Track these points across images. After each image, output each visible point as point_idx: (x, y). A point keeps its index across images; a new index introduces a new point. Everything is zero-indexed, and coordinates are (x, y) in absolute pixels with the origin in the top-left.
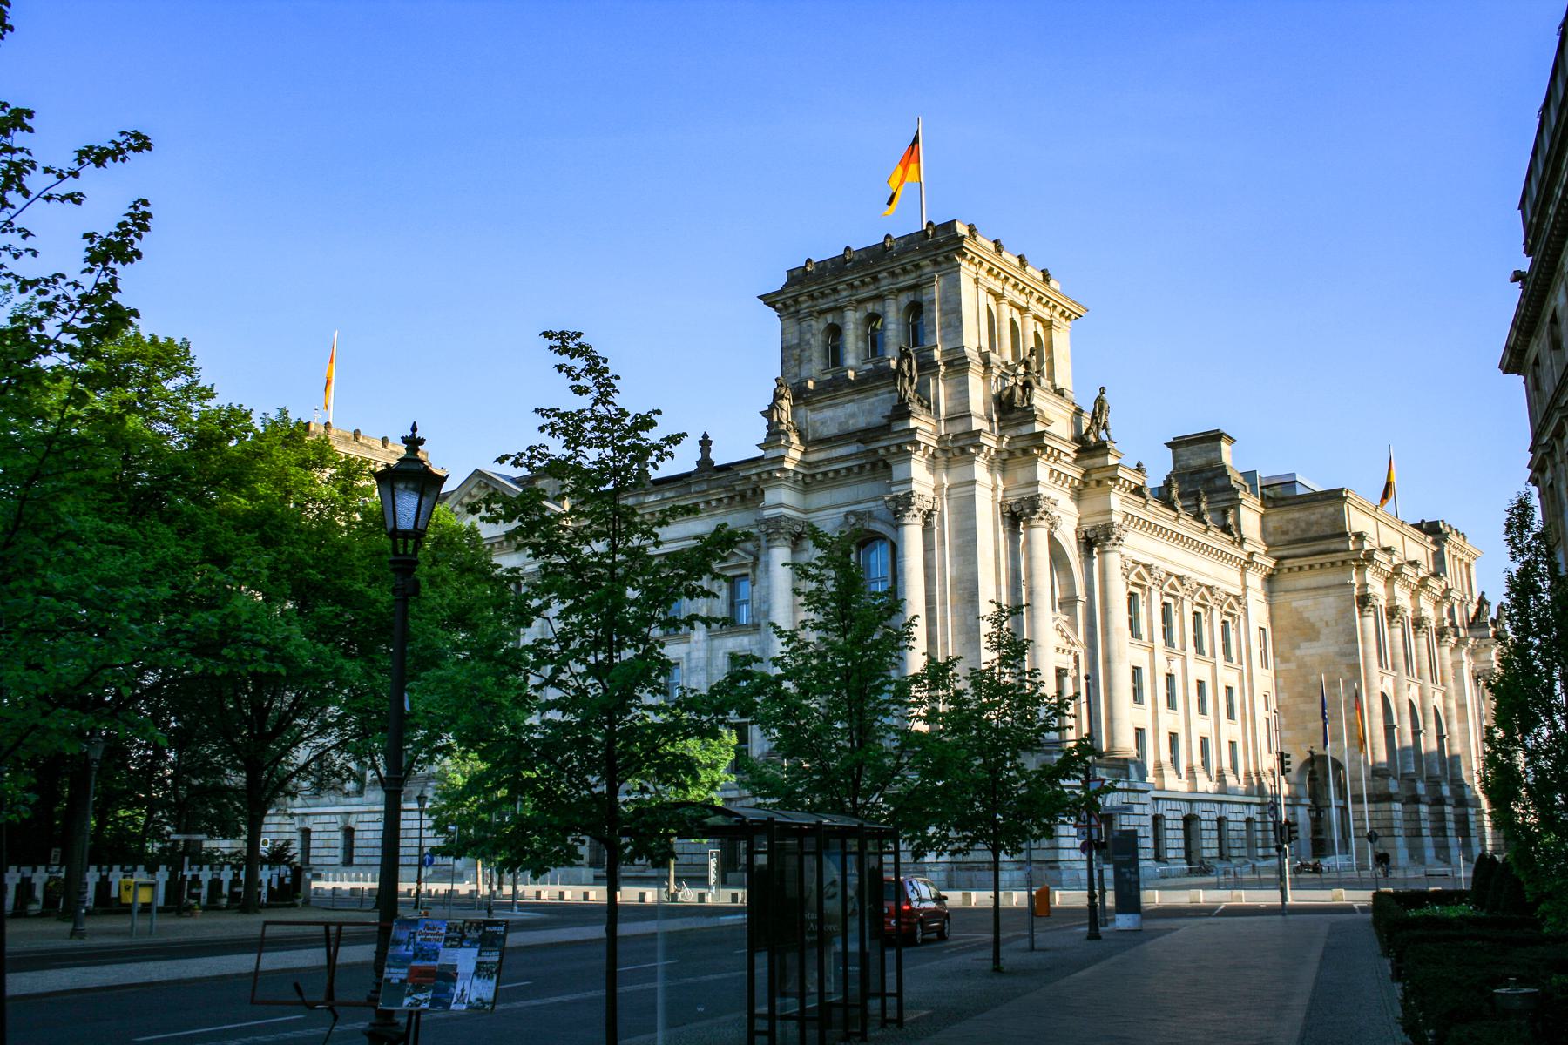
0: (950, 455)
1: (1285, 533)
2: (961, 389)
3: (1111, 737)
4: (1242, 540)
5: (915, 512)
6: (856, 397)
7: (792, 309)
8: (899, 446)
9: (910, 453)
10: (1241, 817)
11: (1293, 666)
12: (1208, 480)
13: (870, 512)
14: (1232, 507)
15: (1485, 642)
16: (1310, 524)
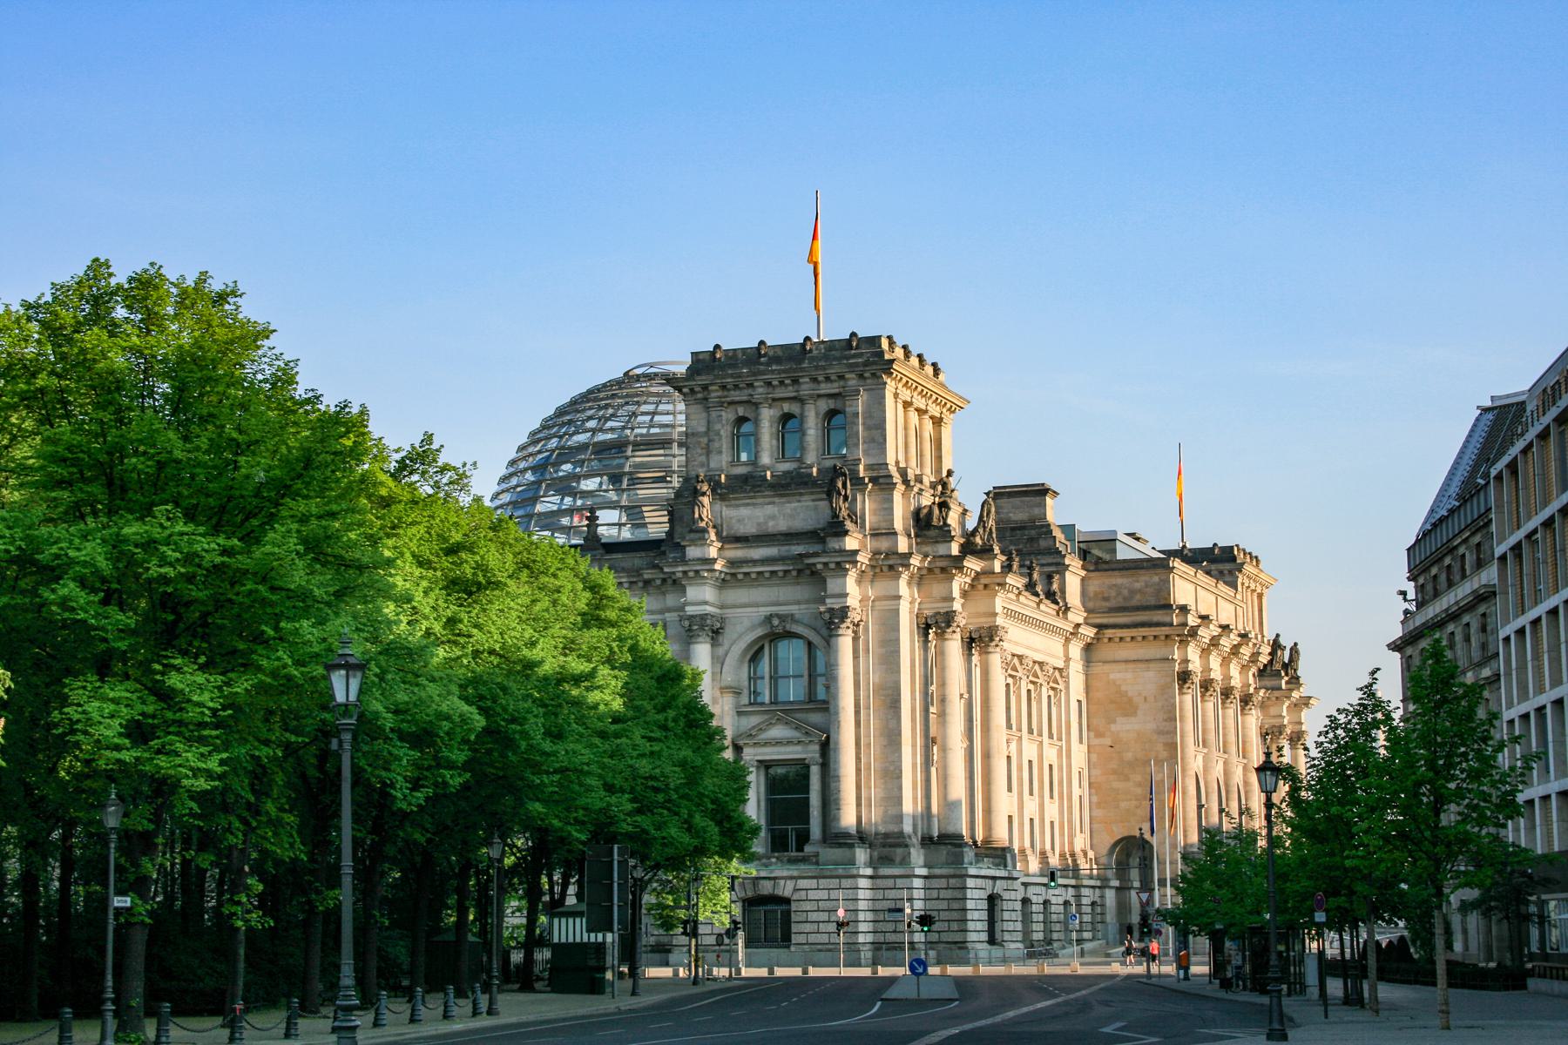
0: (878, 570)
1: (1106, 599)
2: (886, 506)
3: (988, 826)
4: (1067, 609)
6: (776, 500)
7: (700, 396)
8: (838, 564)
9: (847, 570)
10: (1061, 900)
12: (1031, 540)
14: (1057, 572)
15: (1277, 693)
16: (1133, 592)
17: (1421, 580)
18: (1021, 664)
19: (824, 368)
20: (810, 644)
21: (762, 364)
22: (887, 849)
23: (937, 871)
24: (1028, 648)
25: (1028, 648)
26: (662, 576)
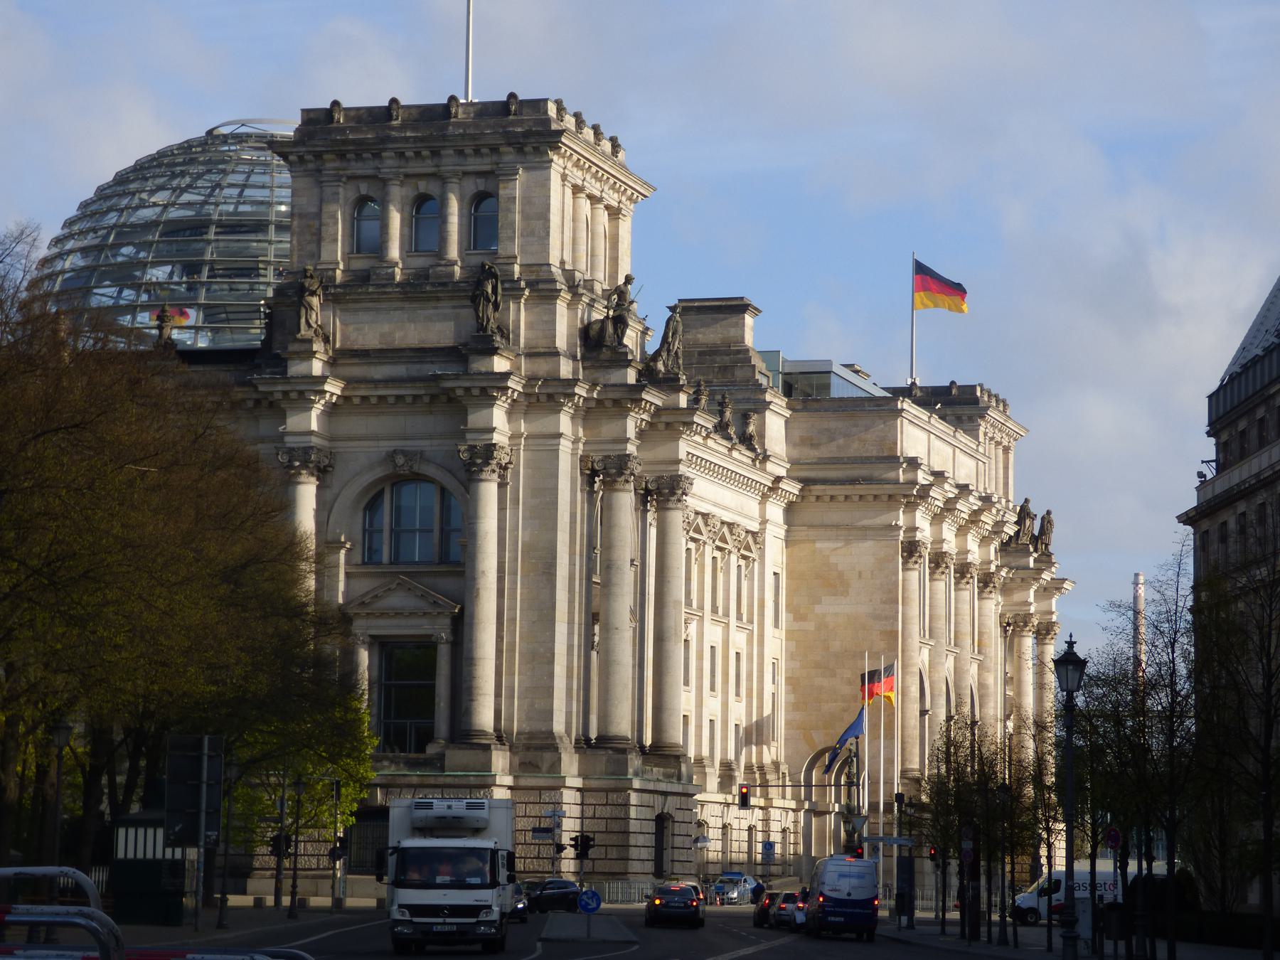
0: (533, 400)
2: (546, 318)
4: (766, 458)
5: (494, 467)
6: (407, 305)
7: (311, 166)
9: (495, 398)
10: (745, 825)
11: (810, 626)
13: (422, 453)
14: (756, 411)
15: (1022, 574)
17: (1224, 437)
18: (706, 525)
20: (443, 490)
24: (715, 504)
25: (715, 504)
26: (255, 396)
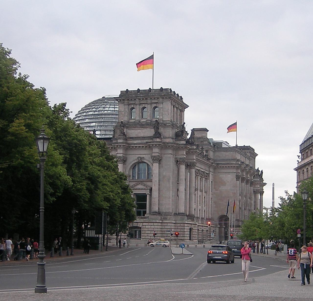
1: (219, 157)
6: (141, 128)
13: (144, 157)
17: (303, 153)
19: (154, 96)
20: (148, 164)
21: (138, 94)
22: (166, 216)
23: (178, 222)
26: (111, 147)
